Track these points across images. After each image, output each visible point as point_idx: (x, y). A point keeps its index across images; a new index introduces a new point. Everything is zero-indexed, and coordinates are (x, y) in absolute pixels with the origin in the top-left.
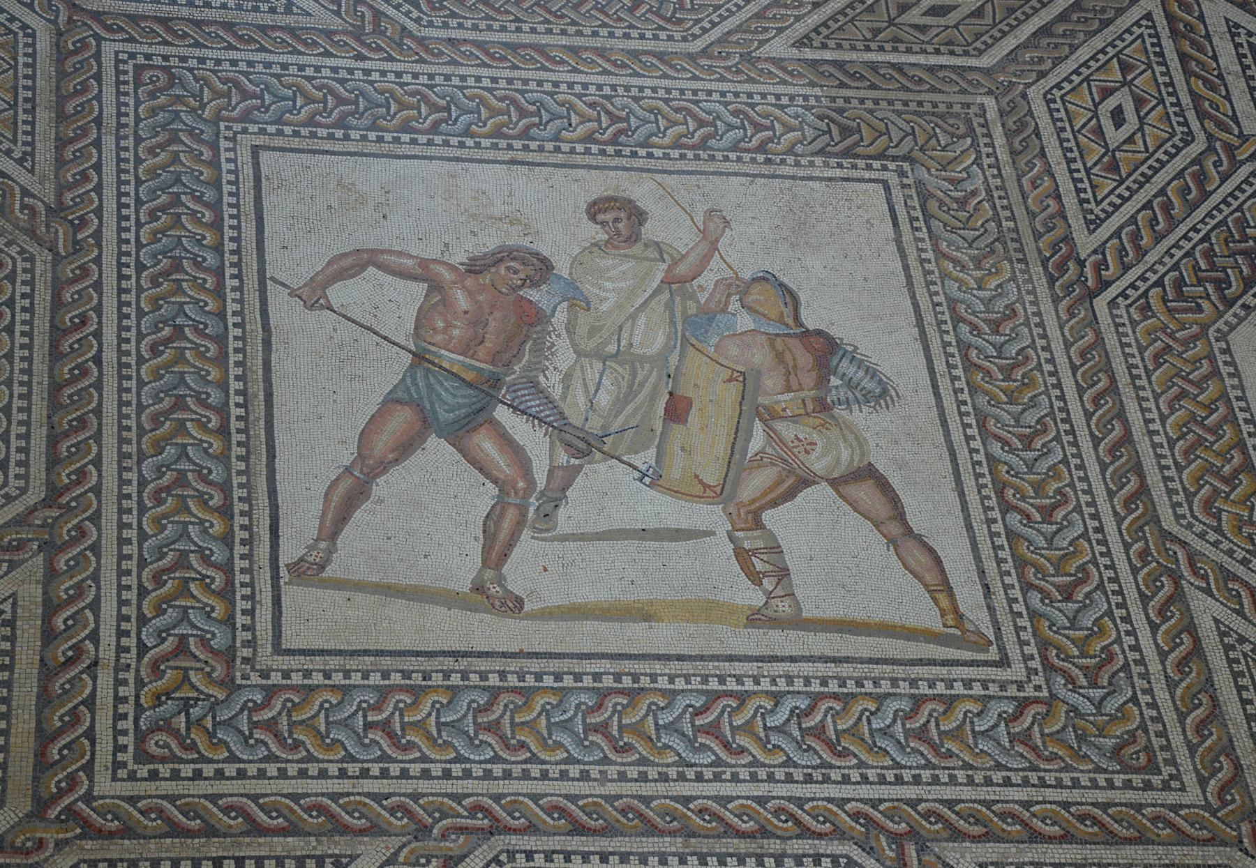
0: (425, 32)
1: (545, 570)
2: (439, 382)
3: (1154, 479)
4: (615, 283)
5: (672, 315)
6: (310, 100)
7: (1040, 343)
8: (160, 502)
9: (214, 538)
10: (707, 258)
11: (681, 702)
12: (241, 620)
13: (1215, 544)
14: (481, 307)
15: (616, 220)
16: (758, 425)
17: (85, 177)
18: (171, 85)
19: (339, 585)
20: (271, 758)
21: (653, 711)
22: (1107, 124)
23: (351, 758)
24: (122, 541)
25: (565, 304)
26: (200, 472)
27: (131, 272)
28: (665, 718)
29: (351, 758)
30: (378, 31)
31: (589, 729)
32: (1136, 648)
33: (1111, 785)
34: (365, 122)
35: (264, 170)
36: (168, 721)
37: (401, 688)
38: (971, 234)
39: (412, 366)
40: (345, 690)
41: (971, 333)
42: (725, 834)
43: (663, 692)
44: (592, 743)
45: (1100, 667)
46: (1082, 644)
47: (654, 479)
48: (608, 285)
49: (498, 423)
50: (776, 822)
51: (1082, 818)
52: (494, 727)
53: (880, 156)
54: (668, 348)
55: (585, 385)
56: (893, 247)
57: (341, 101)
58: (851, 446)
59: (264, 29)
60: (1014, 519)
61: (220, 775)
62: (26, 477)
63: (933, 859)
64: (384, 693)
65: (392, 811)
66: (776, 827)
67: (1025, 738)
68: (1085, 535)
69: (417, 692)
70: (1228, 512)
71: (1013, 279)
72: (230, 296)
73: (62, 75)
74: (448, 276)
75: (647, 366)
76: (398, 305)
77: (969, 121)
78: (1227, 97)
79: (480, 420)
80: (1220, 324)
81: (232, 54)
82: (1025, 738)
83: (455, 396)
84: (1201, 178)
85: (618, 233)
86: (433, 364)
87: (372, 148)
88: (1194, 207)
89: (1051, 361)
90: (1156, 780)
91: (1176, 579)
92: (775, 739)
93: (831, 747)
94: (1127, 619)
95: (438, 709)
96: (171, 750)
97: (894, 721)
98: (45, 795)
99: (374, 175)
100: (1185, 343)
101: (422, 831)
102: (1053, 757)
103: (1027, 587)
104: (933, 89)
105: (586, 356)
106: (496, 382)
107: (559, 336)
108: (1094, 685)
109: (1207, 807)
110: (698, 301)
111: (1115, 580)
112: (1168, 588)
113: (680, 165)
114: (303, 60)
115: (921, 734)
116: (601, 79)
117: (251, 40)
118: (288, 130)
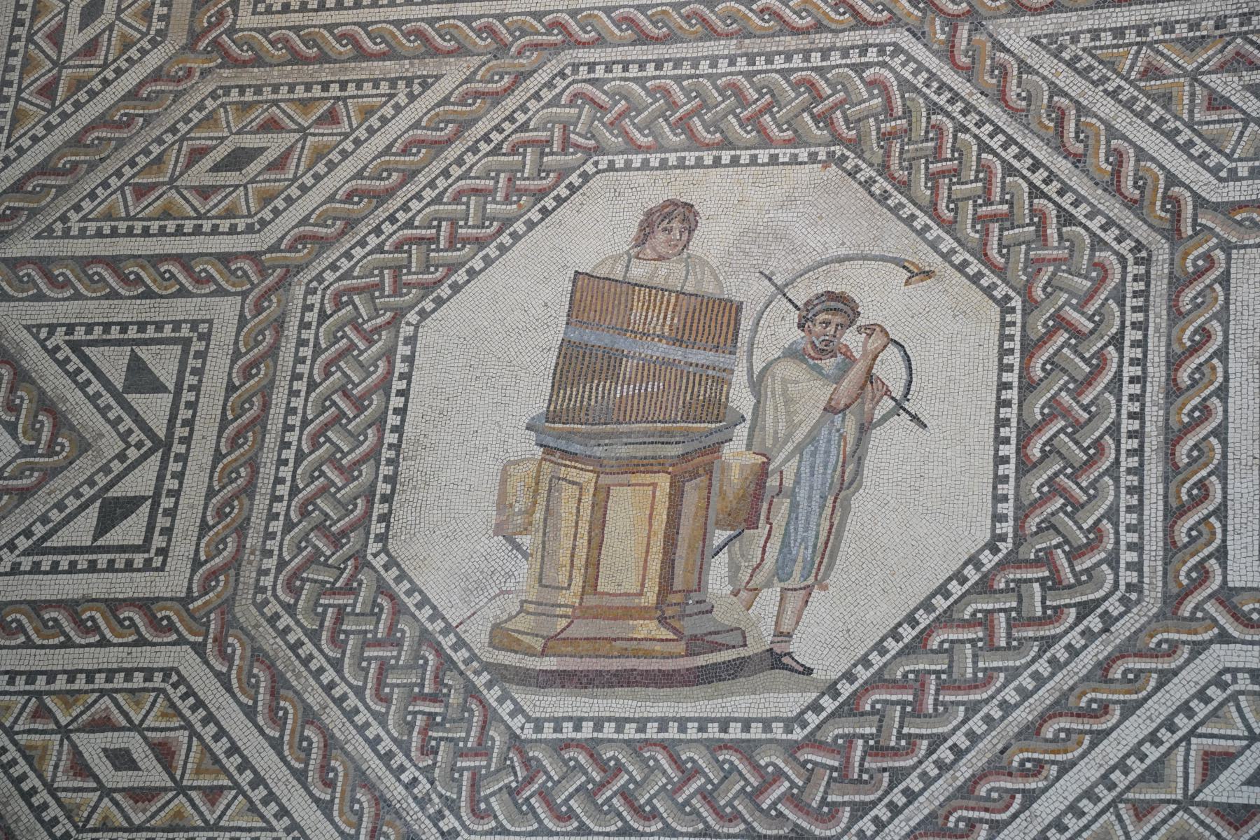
42: (781, 32)
50: (833, 15)
63: (984, 37)
65: (479, 32)
66: (833, 20)
98: (198, 30)
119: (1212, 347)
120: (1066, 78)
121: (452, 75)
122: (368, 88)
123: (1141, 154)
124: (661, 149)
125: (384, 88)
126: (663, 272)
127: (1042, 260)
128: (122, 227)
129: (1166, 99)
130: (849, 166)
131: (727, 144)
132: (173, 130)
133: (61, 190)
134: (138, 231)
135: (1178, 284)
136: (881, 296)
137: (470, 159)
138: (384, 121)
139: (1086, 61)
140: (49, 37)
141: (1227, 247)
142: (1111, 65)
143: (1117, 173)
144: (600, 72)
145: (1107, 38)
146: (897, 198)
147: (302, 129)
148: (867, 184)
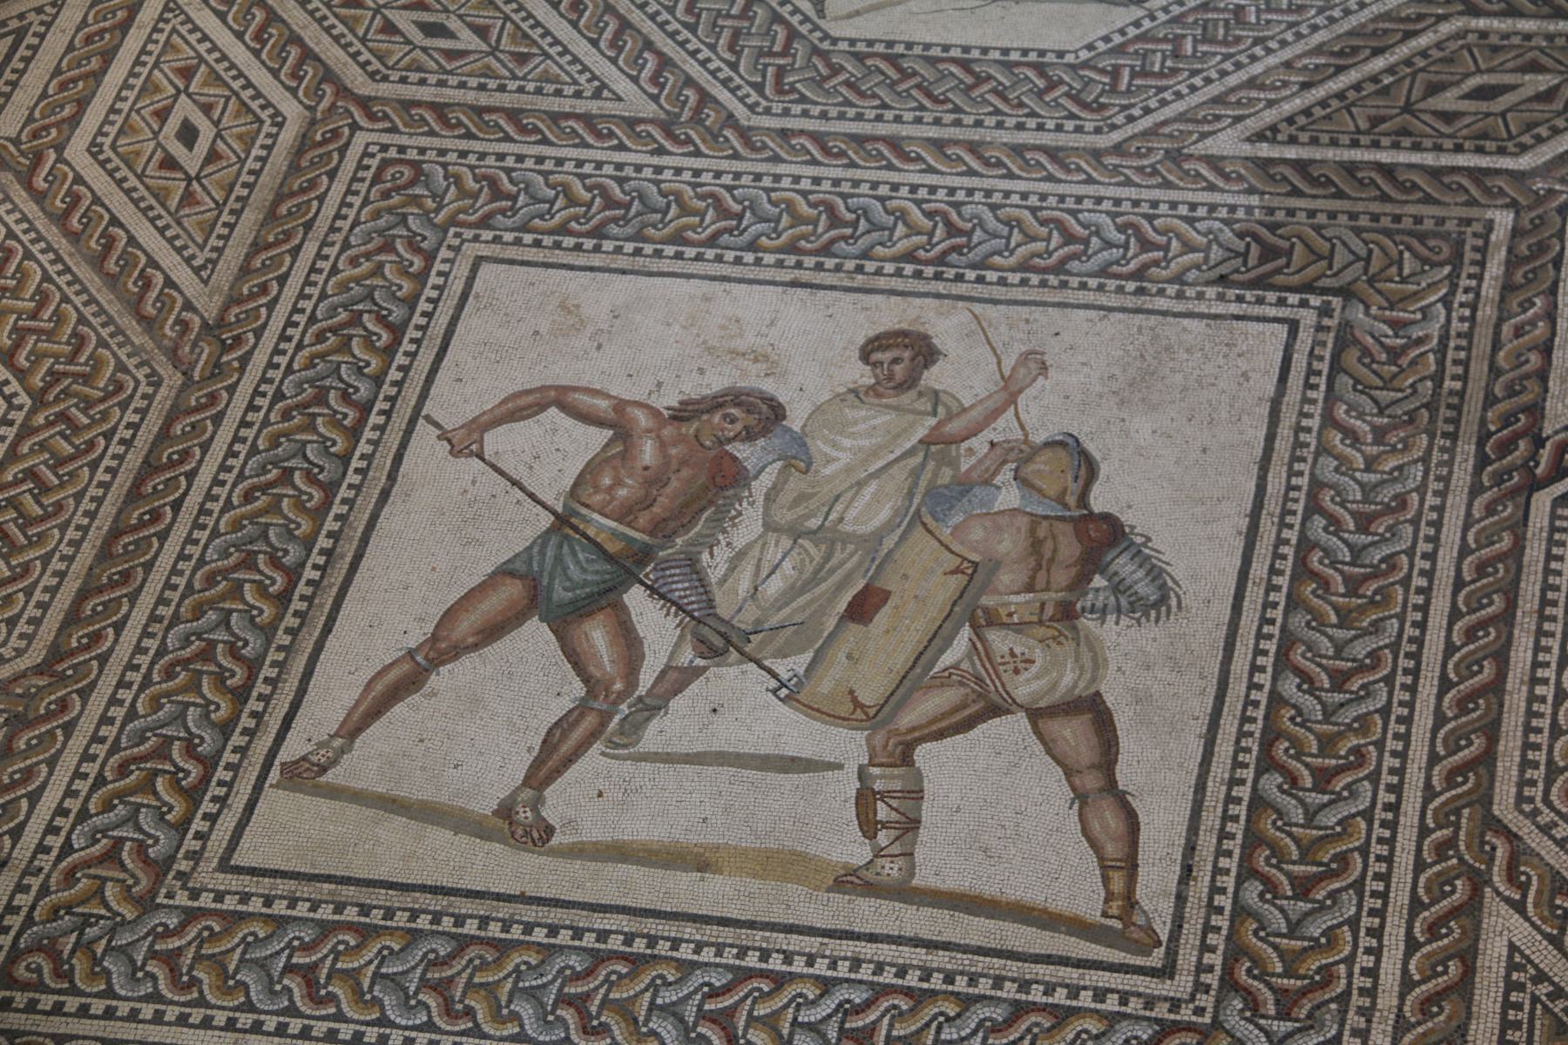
1: (600, 795)
2: (574, 554)
5: (915, 484)
9: (213, 725)
11: (698, 978)
14: (668, 464)
15: (896, 361)
16: (966, 632)
18: (412, 183)
25: (779, 464)
26: (232, 644)
28: (667, 997)
30: (697, 119)
36: (53, 940)
39: (548, 532)
41: (1325, 529)
44: (558, 1018)
47: (790, 693)
48: (847, 443)
49: (625, 609)
54: (889, 527)
55: (758, 567)
56: (1265, 410)
58: (1082, 668)
74: (642, 419)
75: (851, 547)
79: (604, 602)
83: (584, 570)
85: (890, 377)
86: (576, 529)
96: (40, 975)
97: (974, 1032)
99: (601, 295)
105: (775, 530)
106: (643, 555)
107: (752, 504)
110: (957, 468)
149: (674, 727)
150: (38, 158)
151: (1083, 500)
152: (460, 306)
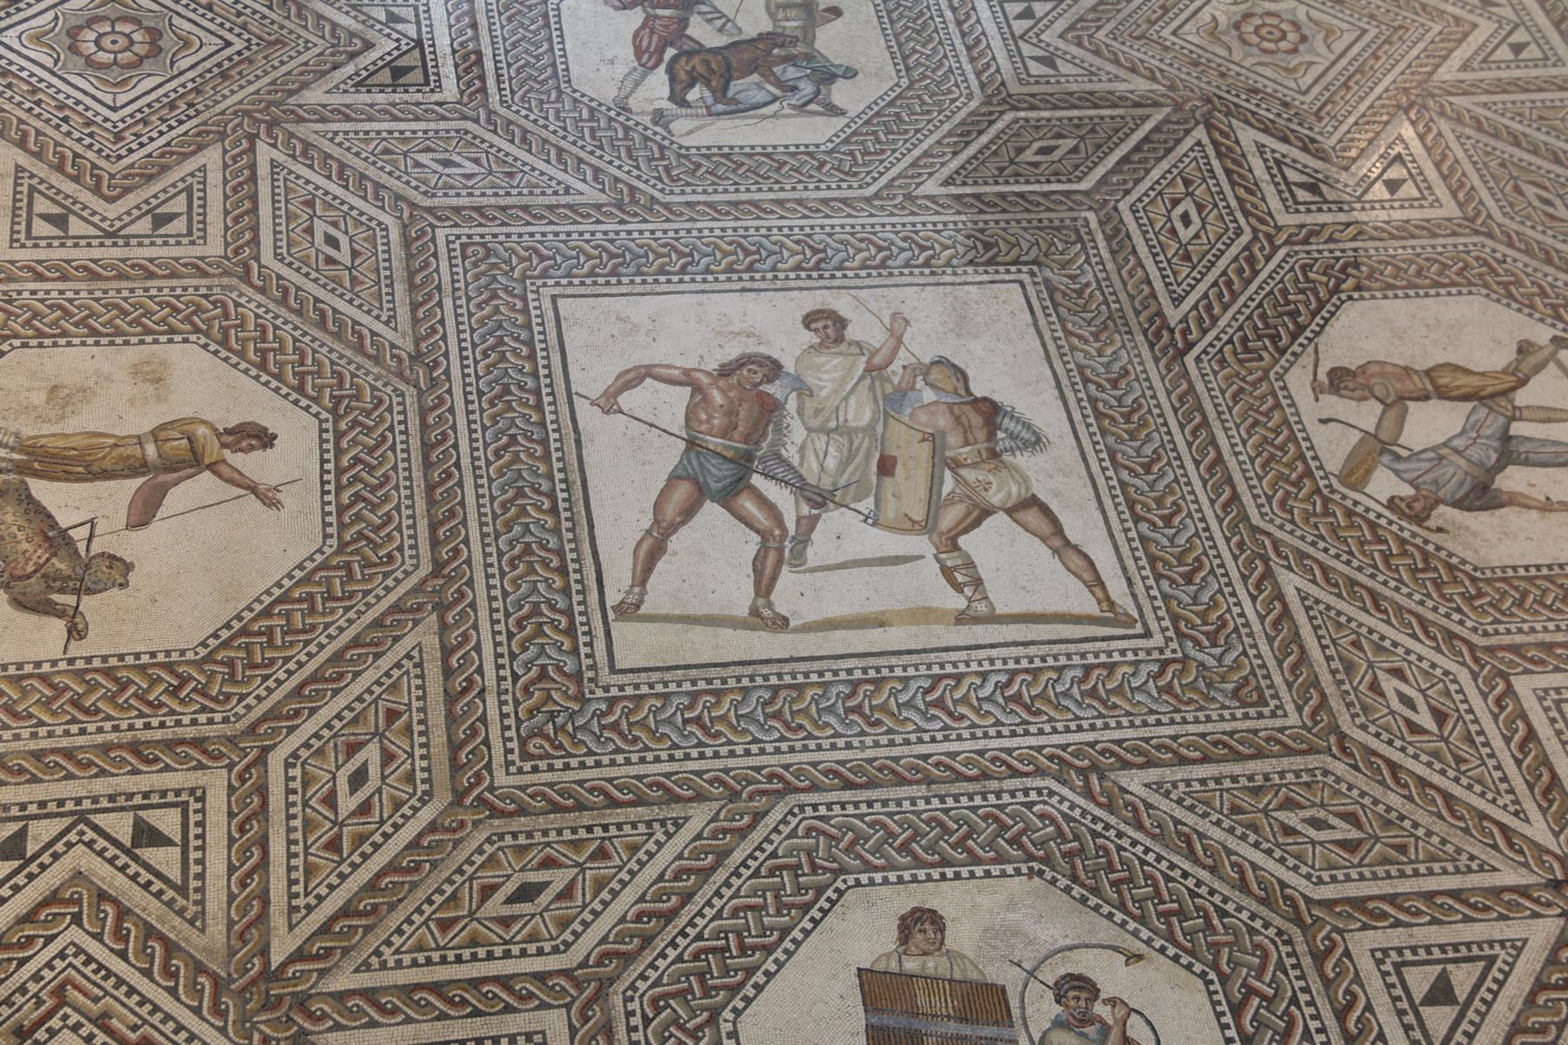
0: (668, 199)
3: (1242, 487)
4: (830, 374)
6: (589, 257)
7: (1148, 393)
8: (515, 567)
10: (895, 351)
11: (914, 685)
12: (583, 650)
13: (1291, 533)
16: (948, 473)
17: (434, 330)
18: (488, 256)
19: (652, 618)
20: (618, 751)
21: (894, 693)
22: (1179, 225)
23: (676, 746)
24: (491, 599)
27: (474, 397)
28: (903, 698)
29: (676, 746)
31: (848, 711)
32: (1242, 615)
33: (1234, 718)
34: (632, 269)
35: (562, 313)
37: (706, 692)
38: (1089, 316)
40: (666, 697)
42: (957, 780)
43: (900, 679)
45: (1217, 631)
46: (1203, 616)
47: (874, 520)
51: (1215, 744)
52: (777, 715)
53: (1016, 262)
54: (874, 421)
56: (1032, 330)
57: (612, 256)
59: (551, 208)
60: (1144, 527)
61: (583, 765)
62: (417, 557)
64: (694, 696)
65: (711, 782)
67: (1169, 690)
68: (1197, 534)
69: (719, 694)
70: (1298, 507)
71: (1124, 346)
72: (548, 409)
73: (410, 256)
74: (705, 380)
76: (671, 404)
77: (1077, 231)
78: (1263, 199)
80: (1277, 368)
81: (530, 229)
82: (1169, 690)
84: (1251, 260)
87: (639, 289)
88: (1248, 282)
89: (1158, 406)
90: (1266, 711)
91: (1266, 561)
92: (986, 706)
93: (1028, 709)
94: (1233, 594)
95: (736, 705)
99: (641, 309)
100: (1254, 384)
101: (734, 795)
102: (1190, 701)
103: (1158, 577)
104: (1049, 210)
106: (749, 457)
108: (1214, 645)
109: (1304, 727)
111: (1222, 566)
112: (1260, 569)
113: (868, 282)
114: (581, 228)
115: (1093, 693)
116: (802, 222)
117: (542, 217)
118: (576, 281)
119: (1362, 1003)
120: (1179, 813)
121: (699, 818)
122: (627, 829)
123: (1255, 867)
124: (894, 868)
125: (642, 828)
126: (931, 964)
127: (1216, 944)
128: (436, 956)
129: (1255, 828)
130: (1049, 875)
131: (945, 862)
132: (460, 871)
133: (368, 929)
134: (451, 958)
135: (1319, 958)
136: (1111, 976)
137: (735, 882)
138: (651, 855)
139: (1188, 802)
140: (324, 801)
141: (1341, 932)
142: (1207, 803)
143: (1243, 879)
144: (823, 811)
145: (1197, 786)
146: (1093, 901)
147: (578, 865)
148: (1067, 890)
149: (817, 552)
150: (248, 269)
151: (969, 393)
152: (559, 326)
